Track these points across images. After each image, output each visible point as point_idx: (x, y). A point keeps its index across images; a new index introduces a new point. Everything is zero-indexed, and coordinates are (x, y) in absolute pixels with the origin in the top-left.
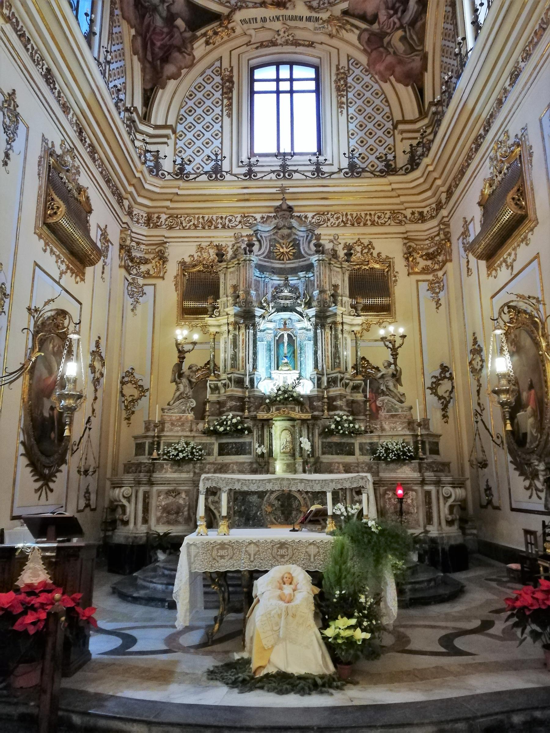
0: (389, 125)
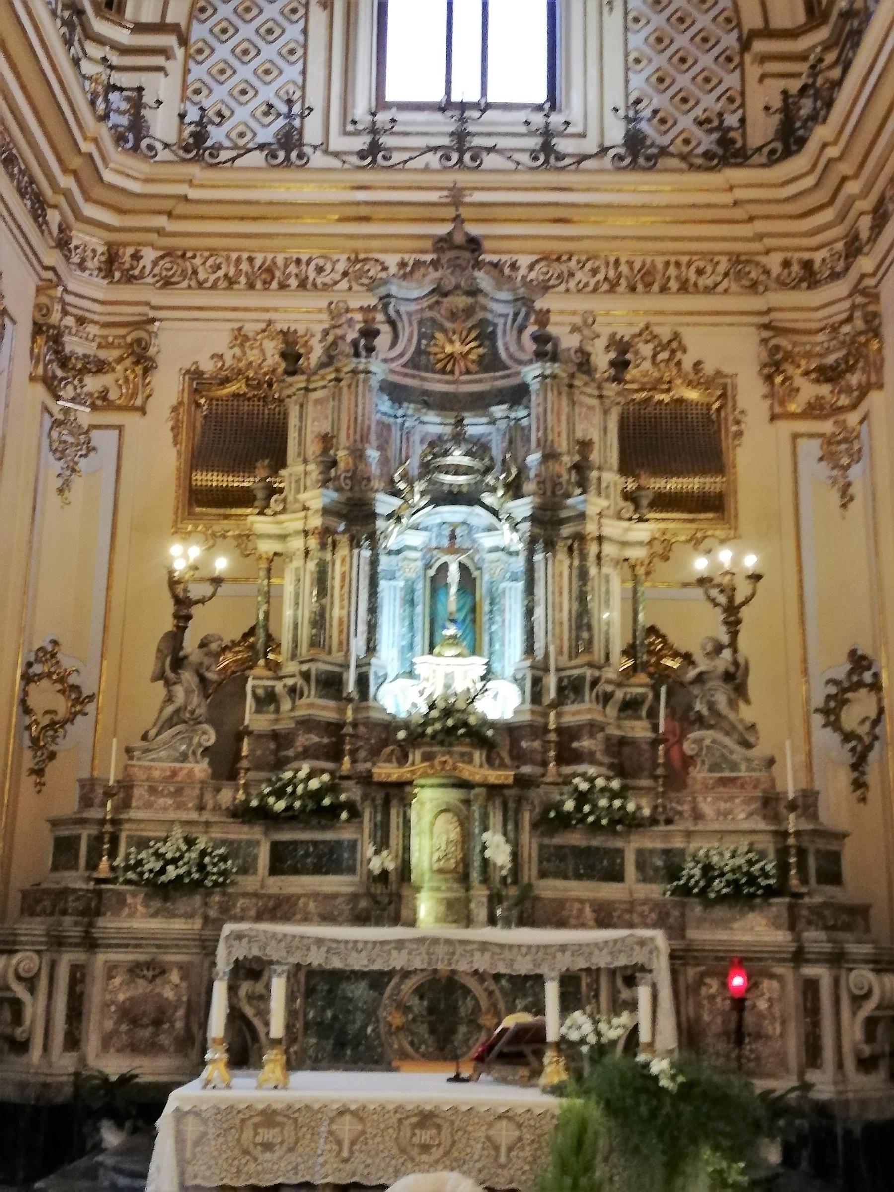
0: (730, 40)
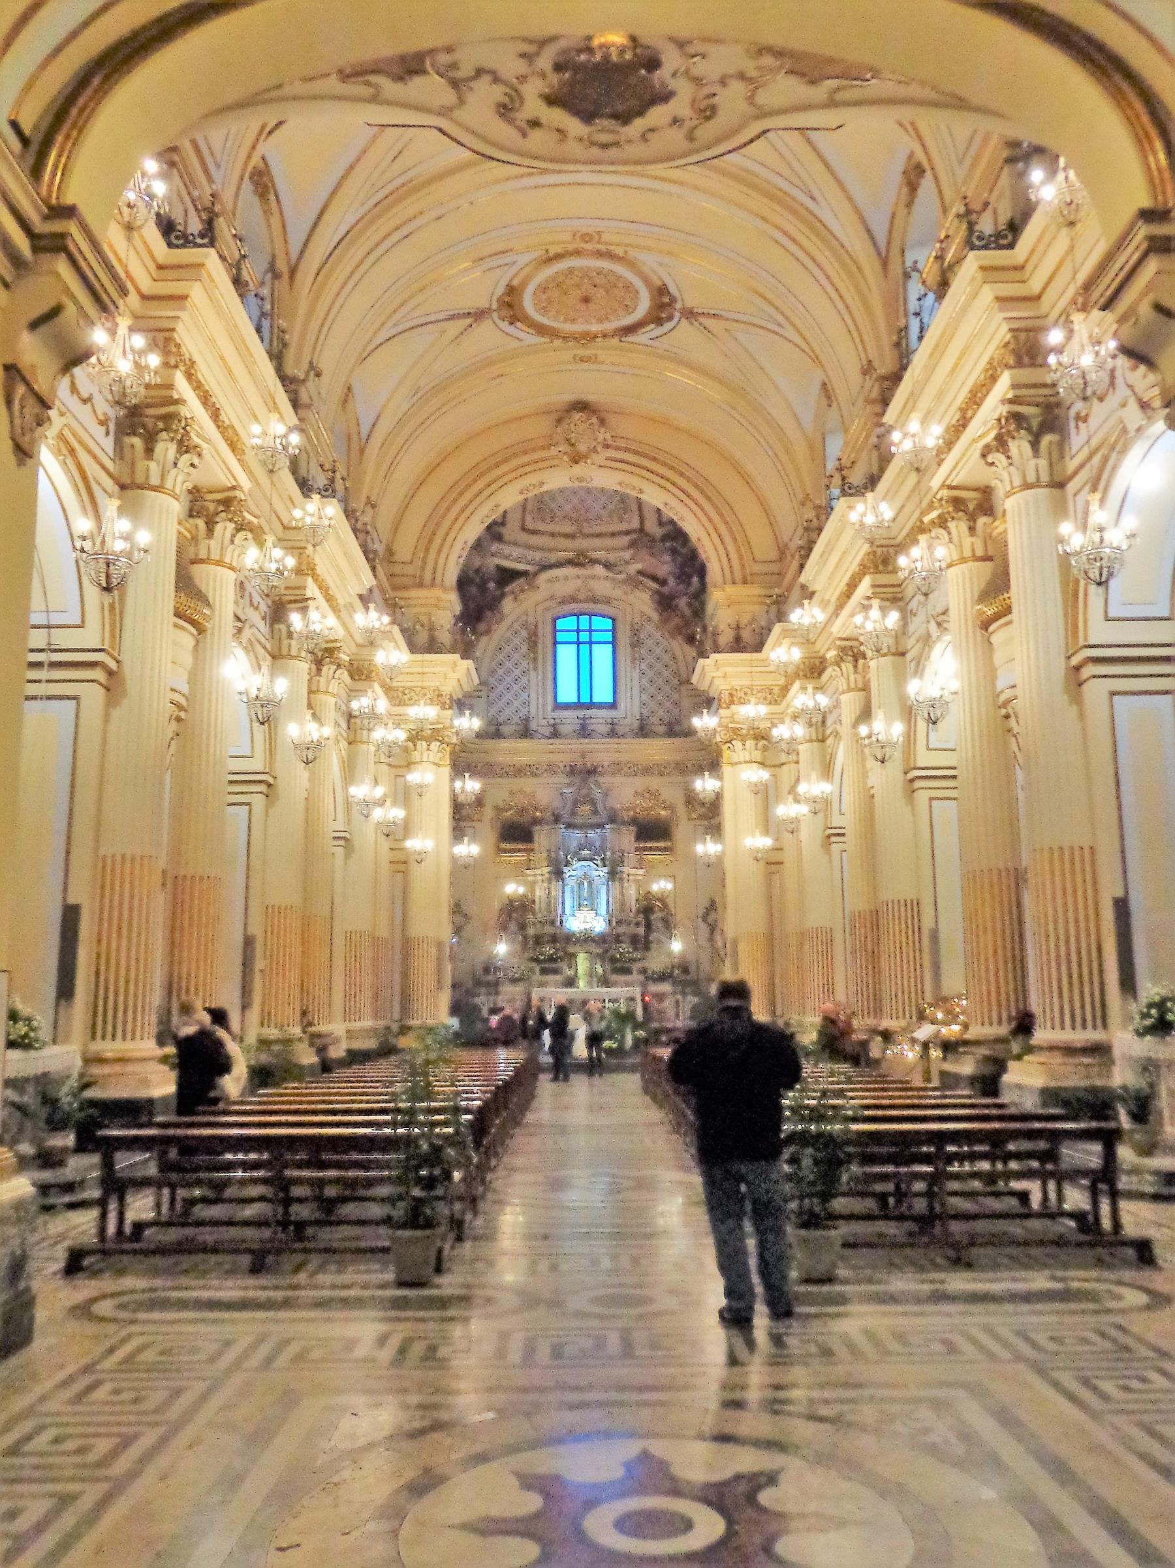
0: (676, 681)
